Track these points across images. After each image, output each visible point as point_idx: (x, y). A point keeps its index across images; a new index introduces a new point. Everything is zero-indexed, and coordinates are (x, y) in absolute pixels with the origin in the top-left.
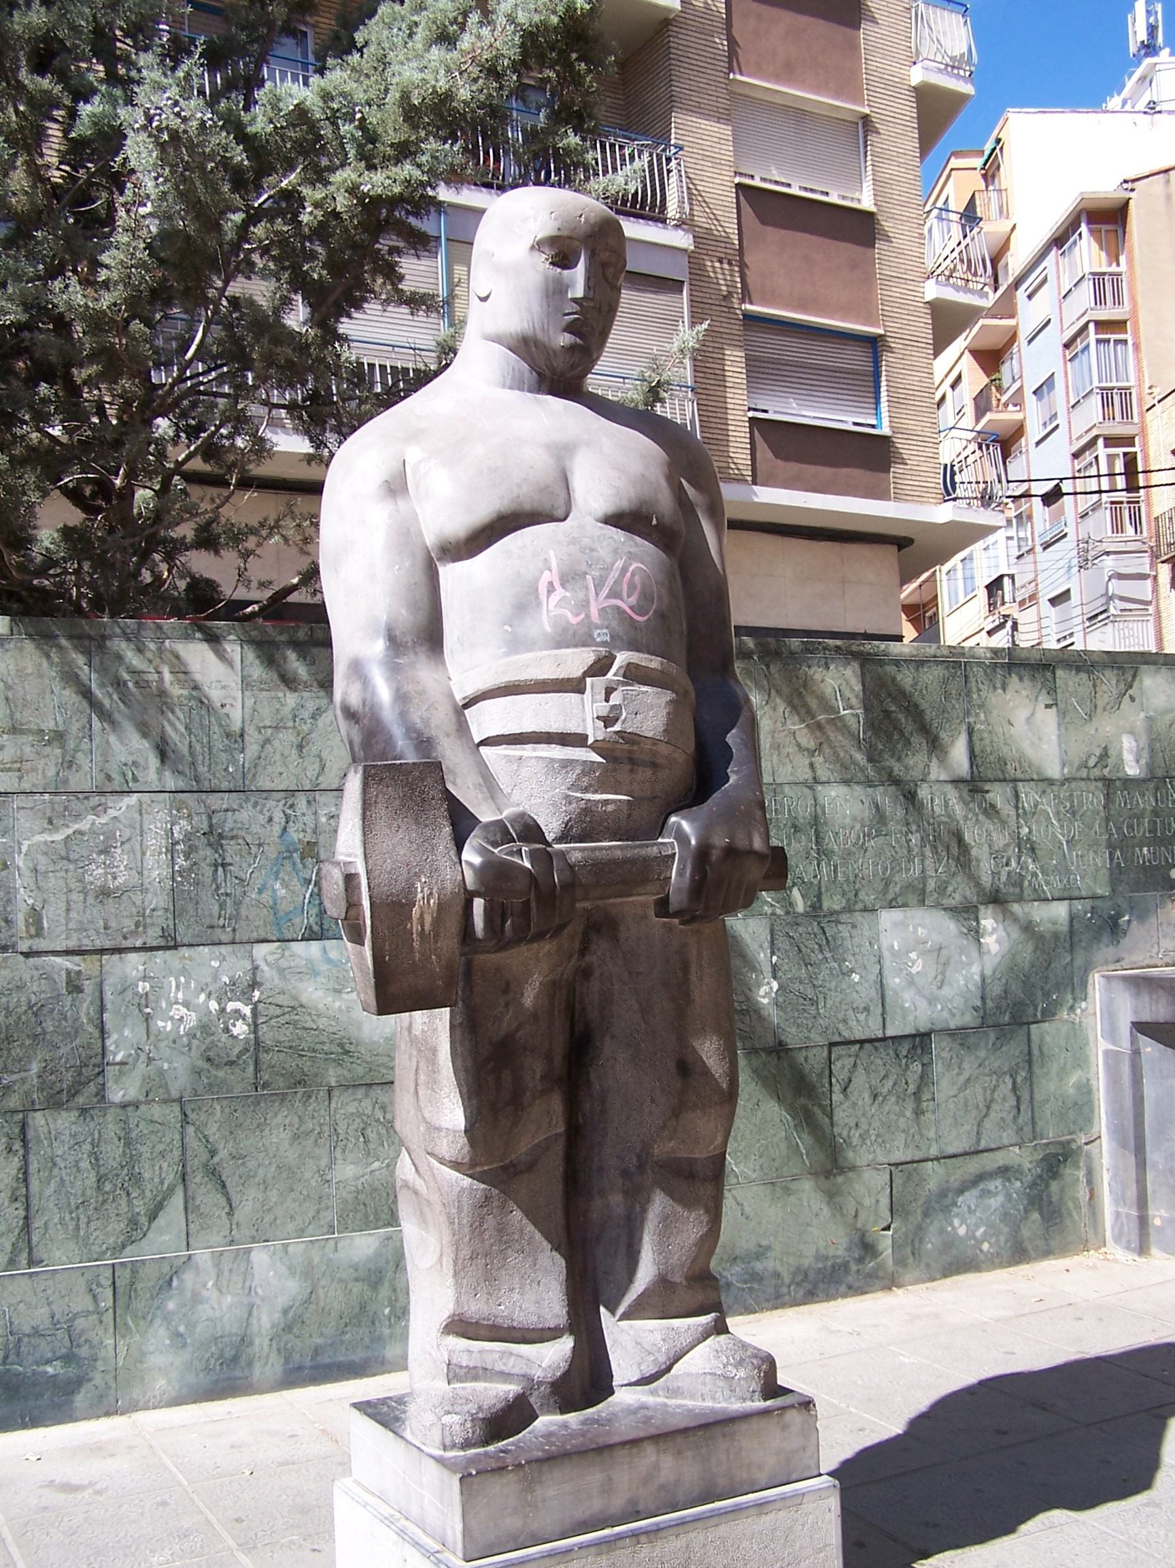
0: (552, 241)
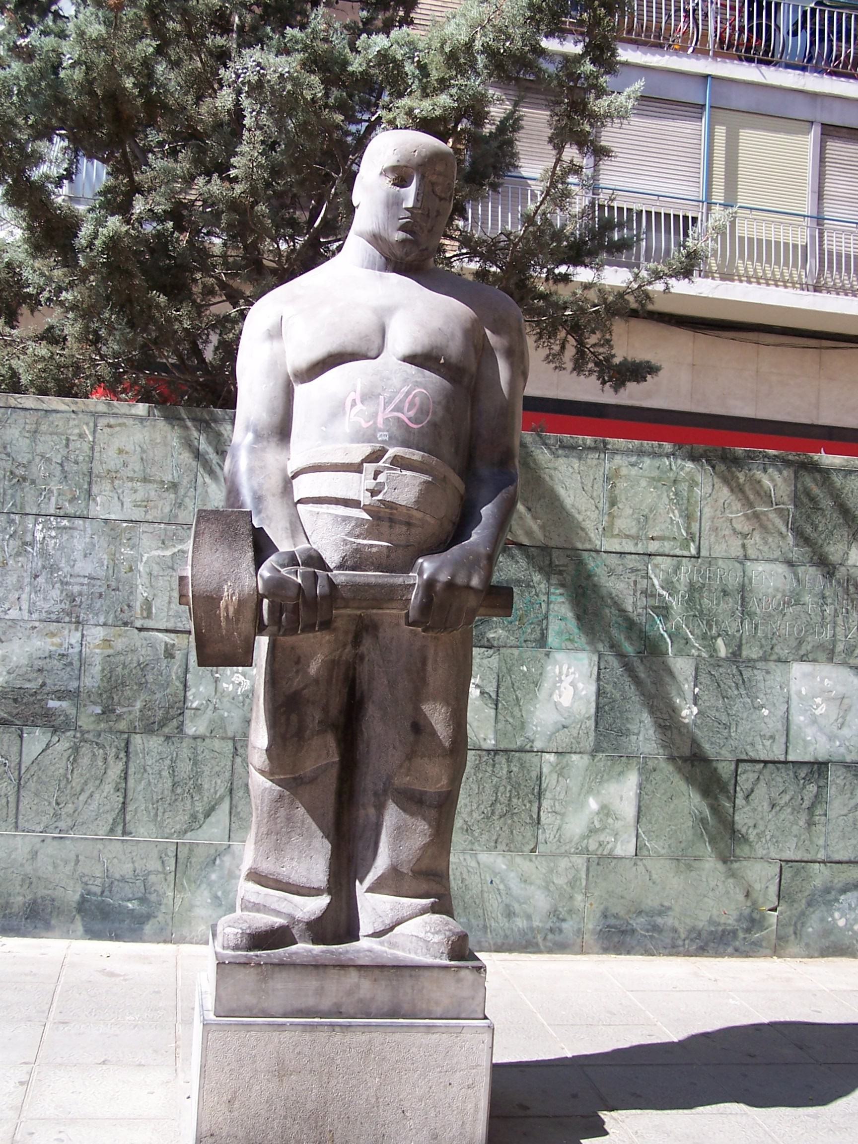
0: (394, 169)
